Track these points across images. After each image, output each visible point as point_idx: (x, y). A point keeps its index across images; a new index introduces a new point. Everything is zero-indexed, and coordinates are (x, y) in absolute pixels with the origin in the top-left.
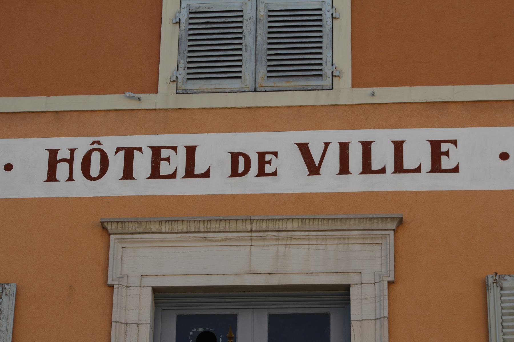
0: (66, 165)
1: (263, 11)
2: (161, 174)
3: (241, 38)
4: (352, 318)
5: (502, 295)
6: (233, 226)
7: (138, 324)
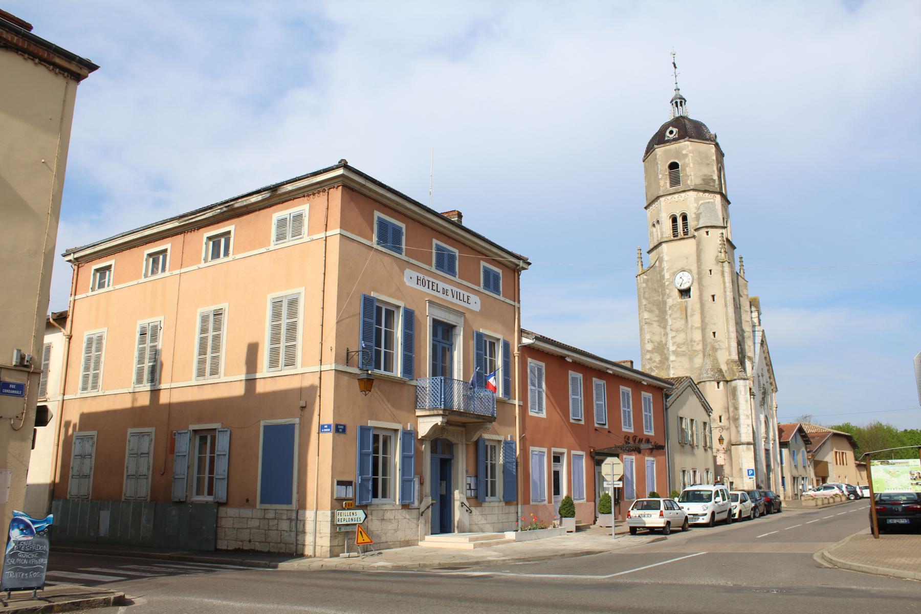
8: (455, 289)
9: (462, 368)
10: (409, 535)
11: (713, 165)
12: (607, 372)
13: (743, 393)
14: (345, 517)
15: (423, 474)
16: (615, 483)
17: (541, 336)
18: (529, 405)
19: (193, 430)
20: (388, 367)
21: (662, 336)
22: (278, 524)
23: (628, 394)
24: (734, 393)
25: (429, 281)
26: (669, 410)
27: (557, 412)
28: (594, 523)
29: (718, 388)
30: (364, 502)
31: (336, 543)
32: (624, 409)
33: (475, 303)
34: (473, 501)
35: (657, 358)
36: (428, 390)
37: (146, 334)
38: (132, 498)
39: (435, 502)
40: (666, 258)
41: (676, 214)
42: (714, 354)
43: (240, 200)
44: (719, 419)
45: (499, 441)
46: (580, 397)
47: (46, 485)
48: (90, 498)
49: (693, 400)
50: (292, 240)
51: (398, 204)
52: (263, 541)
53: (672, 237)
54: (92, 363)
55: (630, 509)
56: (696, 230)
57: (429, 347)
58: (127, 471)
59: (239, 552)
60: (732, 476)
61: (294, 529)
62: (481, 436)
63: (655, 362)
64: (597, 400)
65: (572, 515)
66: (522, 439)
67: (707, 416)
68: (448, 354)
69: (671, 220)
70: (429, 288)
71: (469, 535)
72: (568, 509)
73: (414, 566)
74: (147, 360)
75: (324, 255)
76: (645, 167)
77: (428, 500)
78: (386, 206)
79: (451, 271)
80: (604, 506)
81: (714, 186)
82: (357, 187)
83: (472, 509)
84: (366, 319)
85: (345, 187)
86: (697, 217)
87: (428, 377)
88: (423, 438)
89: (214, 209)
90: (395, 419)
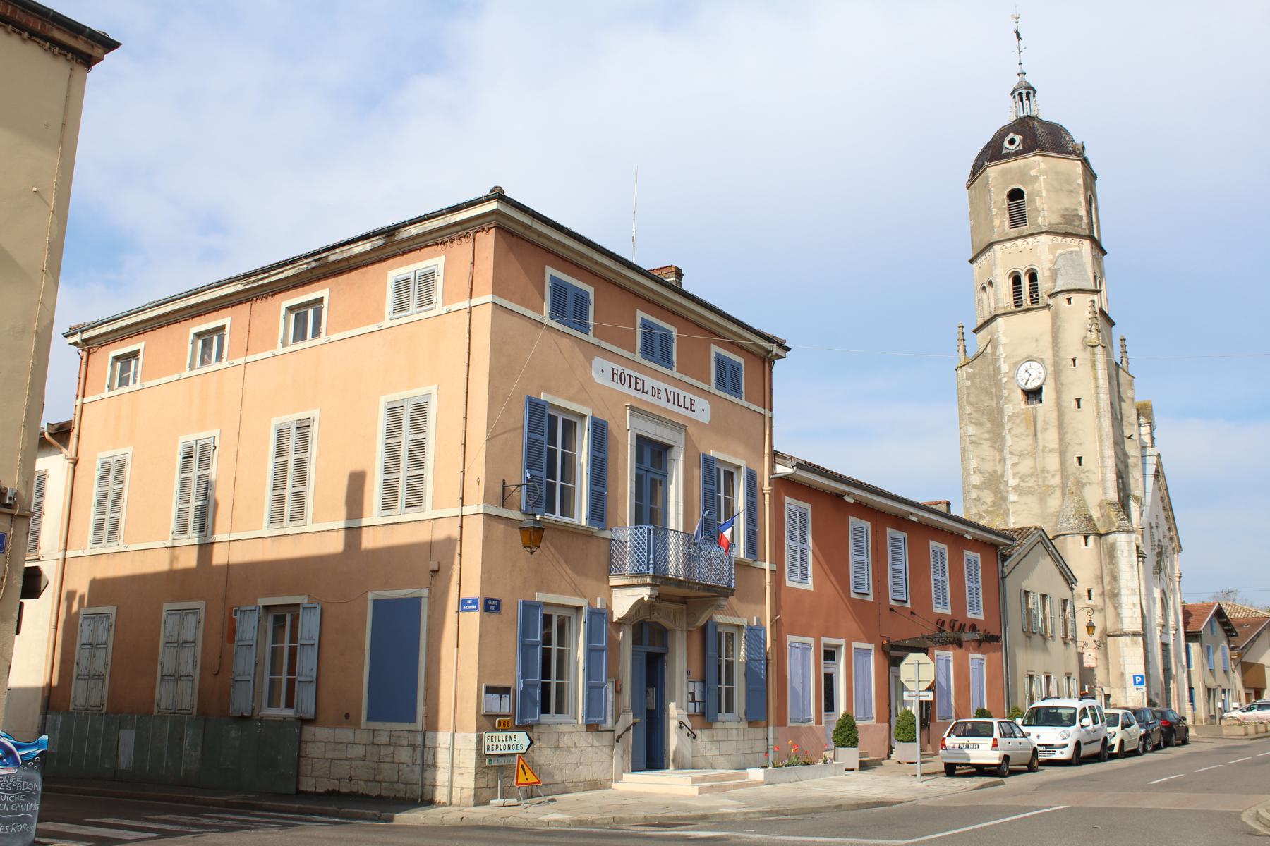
8: (671, 389)
9: (681, 512)
10: (599, 774)
11: (1078, 193)
12: (910, 520)
13: (1126, 553)
14: (499, 743)
15: (621, 678)
16: (921, 693)
17: (805, 462)
18: (787, 570)
19: (264, 606)
20: (567, 510)
21: (997, 464)
22: (393, 754)
23: (942, 554)
24: (1111, 554)
26: (1007, 580)
27: (831, 581)
28: (889, 757)
29: (1086, 545)
30: (528, 720)
31: (483, 783)
32: (937, 577)
33: (703, 411)
34: (698, 720)
35: (988, 497)
36: (628, 545)
37: (192, 457)
38: (169, 711)
39: (638, 720)
40: (1003, 340)
41: (1020, 271)
42: (1079, 493)
43: (337, 250)
44: (1086, 594)
45: (740, 627)
46: (867, 558)
47: (37, 689)
48: (105, 710)
49: (1046, 564)
50: (419, 313)
51: (582, 255)
52: (372, 779)
53: (1013, 308)
54: (109, 502)
55: (945, 736)
56: (1051, 296)
57: (631, 479)
58: (162, 668)
59: (333, 795)
60: (1108, 685)
61: (419, 761)
62: (711, 618)
63: (985, 503)
64: (893, 563)
65: (854, 743)
66: (776, 624)
67: (1068, 589)
68: (660, 489)
69: (1011, 279)
70: (630, 387)
71: (692, 772)
72: (847, 734)
73: (606, 821)
74: (193, 497)
75: (468, 336)
76: (971, 197)
77: (628, 718)
78: (563, 259)
79: (666, 360)
80: (904, 730)
81: (1080, 226)
82: (519, 230)
83: (697, 732)
84: (533, 436)
85: (500, 229)
86: (1052, 276)
87: (628, 525)
88: (621, 621)
89: (298, 264)
90: (577, 591)
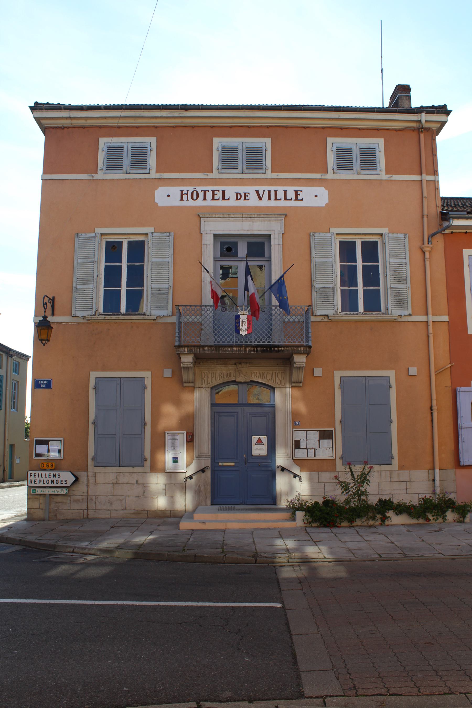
0: (186, 195)
1: (244, 147)
2: (215, 199)
3: (238, 156)
4: (272, 244)
5: (315, 238)
6: (237, 216)
7: (210, 245)
14: (42, 479)
25: (205, 192)
39: (233, 464)
70: (205, 199)
